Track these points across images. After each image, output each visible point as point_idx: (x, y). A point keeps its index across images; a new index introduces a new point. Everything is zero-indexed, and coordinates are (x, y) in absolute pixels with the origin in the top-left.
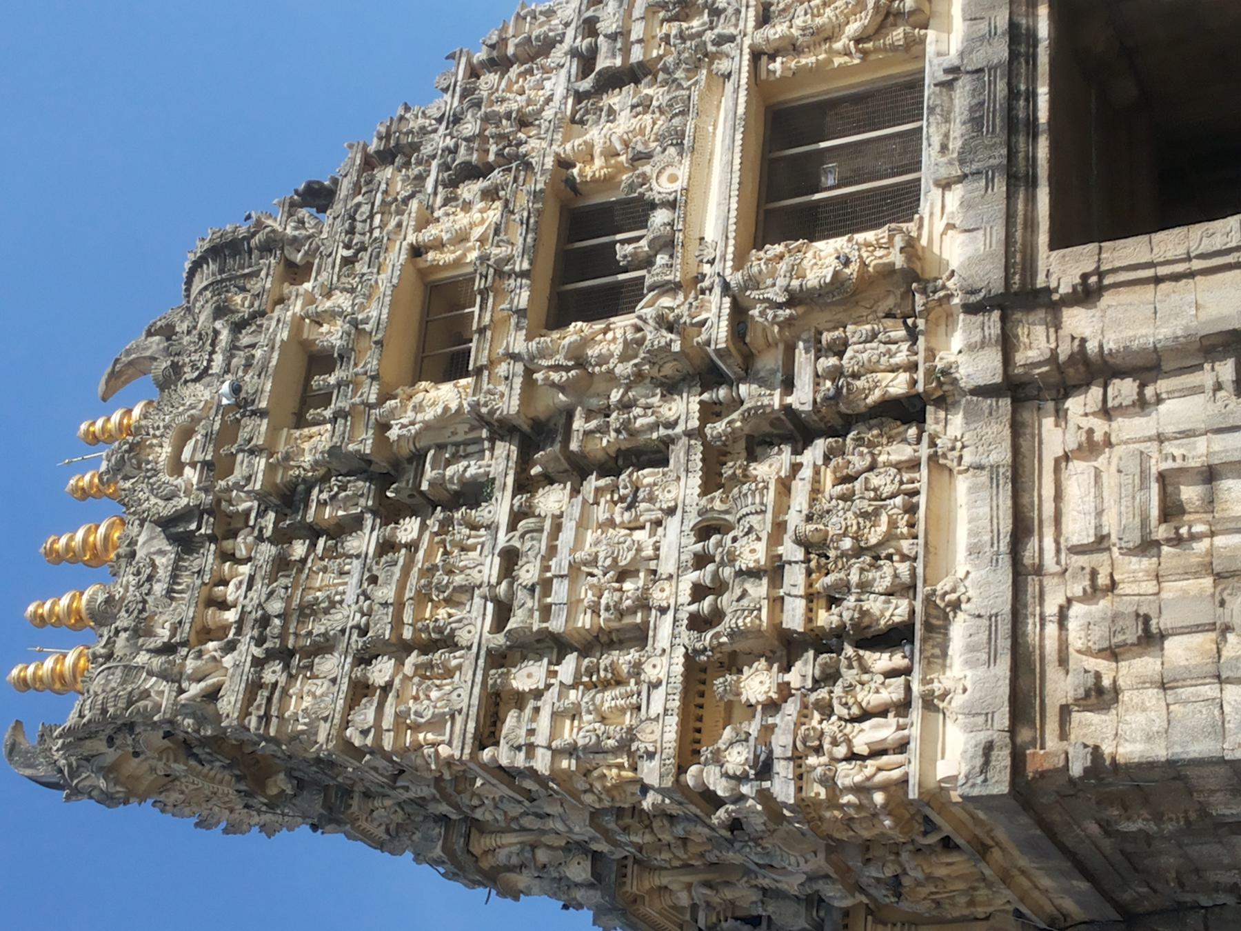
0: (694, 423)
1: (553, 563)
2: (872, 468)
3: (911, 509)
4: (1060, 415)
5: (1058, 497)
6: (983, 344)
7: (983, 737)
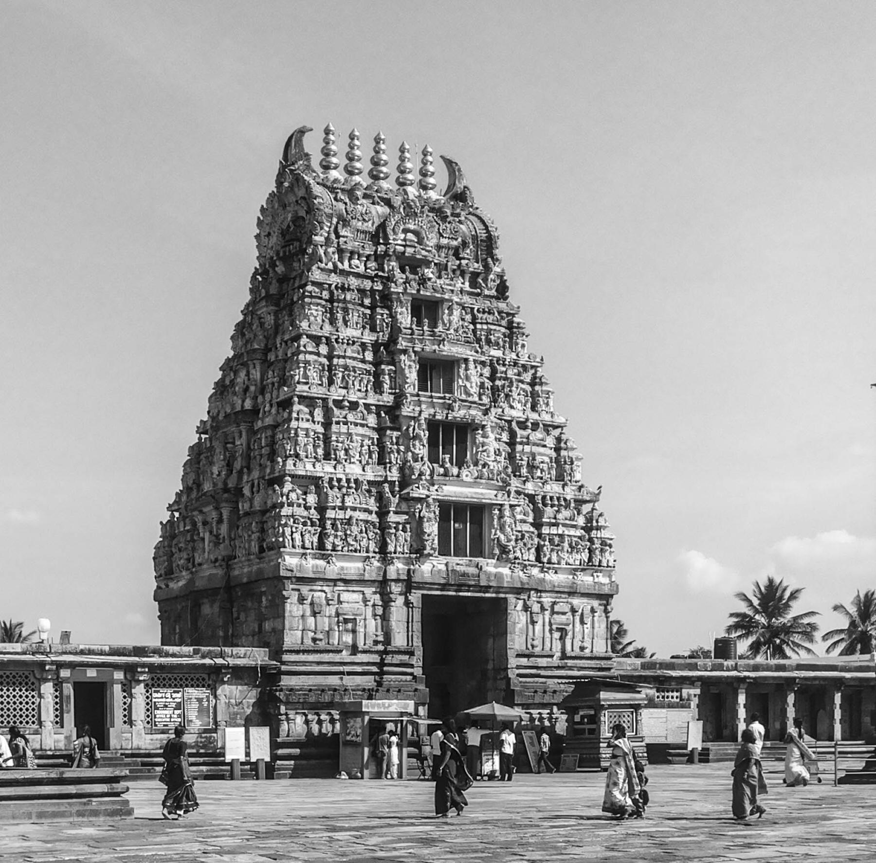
0: (389, 479)
1: (353, 426)
2: (369, 539)
3: (356, 551)
4: (375, 593)
5: (353, 591)
6: (398, 574)
7: (295, 570)
